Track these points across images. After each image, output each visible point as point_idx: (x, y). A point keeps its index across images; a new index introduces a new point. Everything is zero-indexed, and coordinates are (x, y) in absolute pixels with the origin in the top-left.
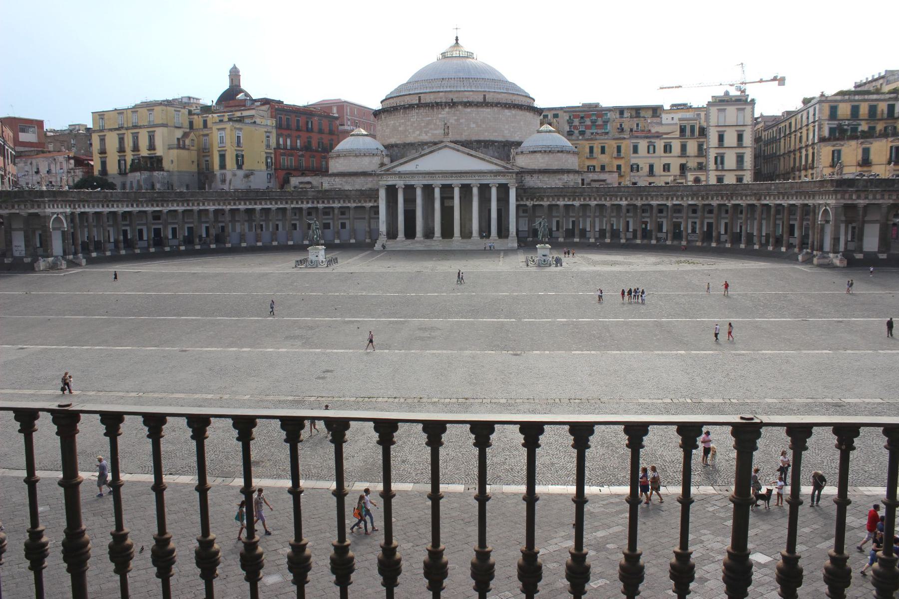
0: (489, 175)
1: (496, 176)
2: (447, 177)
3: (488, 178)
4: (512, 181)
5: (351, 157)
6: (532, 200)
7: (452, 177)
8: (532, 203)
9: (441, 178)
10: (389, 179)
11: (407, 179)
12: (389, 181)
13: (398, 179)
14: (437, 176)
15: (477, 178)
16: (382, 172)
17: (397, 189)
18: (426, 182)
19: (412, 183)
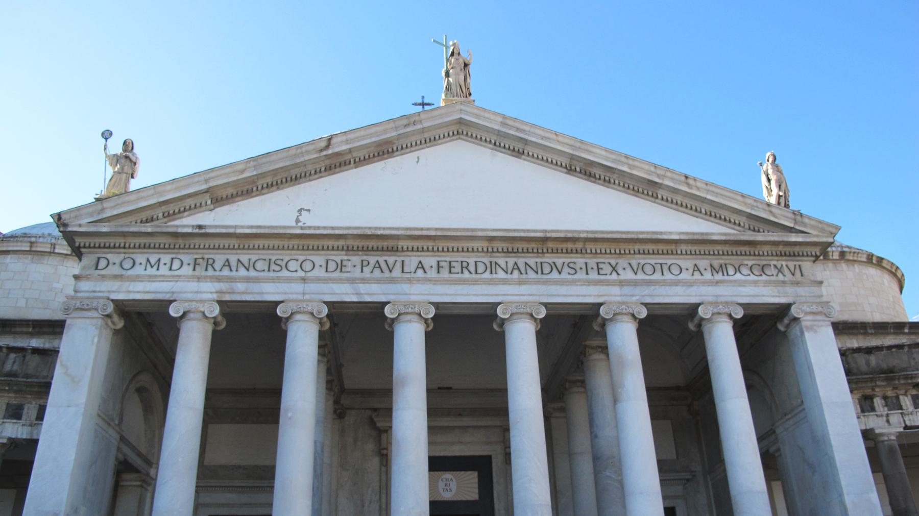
0: (687, 263)
1: (722, 268)
2: (464, 267)
3: (685, 276)
4: (801, 291)
5: (8, 259)
6: (894, 404)
7: (492, 267)
8: (895, 418)
9: (432, 274)
10: (139, 270)
11: (243, 272)
12: (137, 278)
13: (187, 270)
14: (412, 262)
15: (628, 275)
16: (104, 228)
17: (173, 327)
18: (346, 293)
19: (268, 292)
